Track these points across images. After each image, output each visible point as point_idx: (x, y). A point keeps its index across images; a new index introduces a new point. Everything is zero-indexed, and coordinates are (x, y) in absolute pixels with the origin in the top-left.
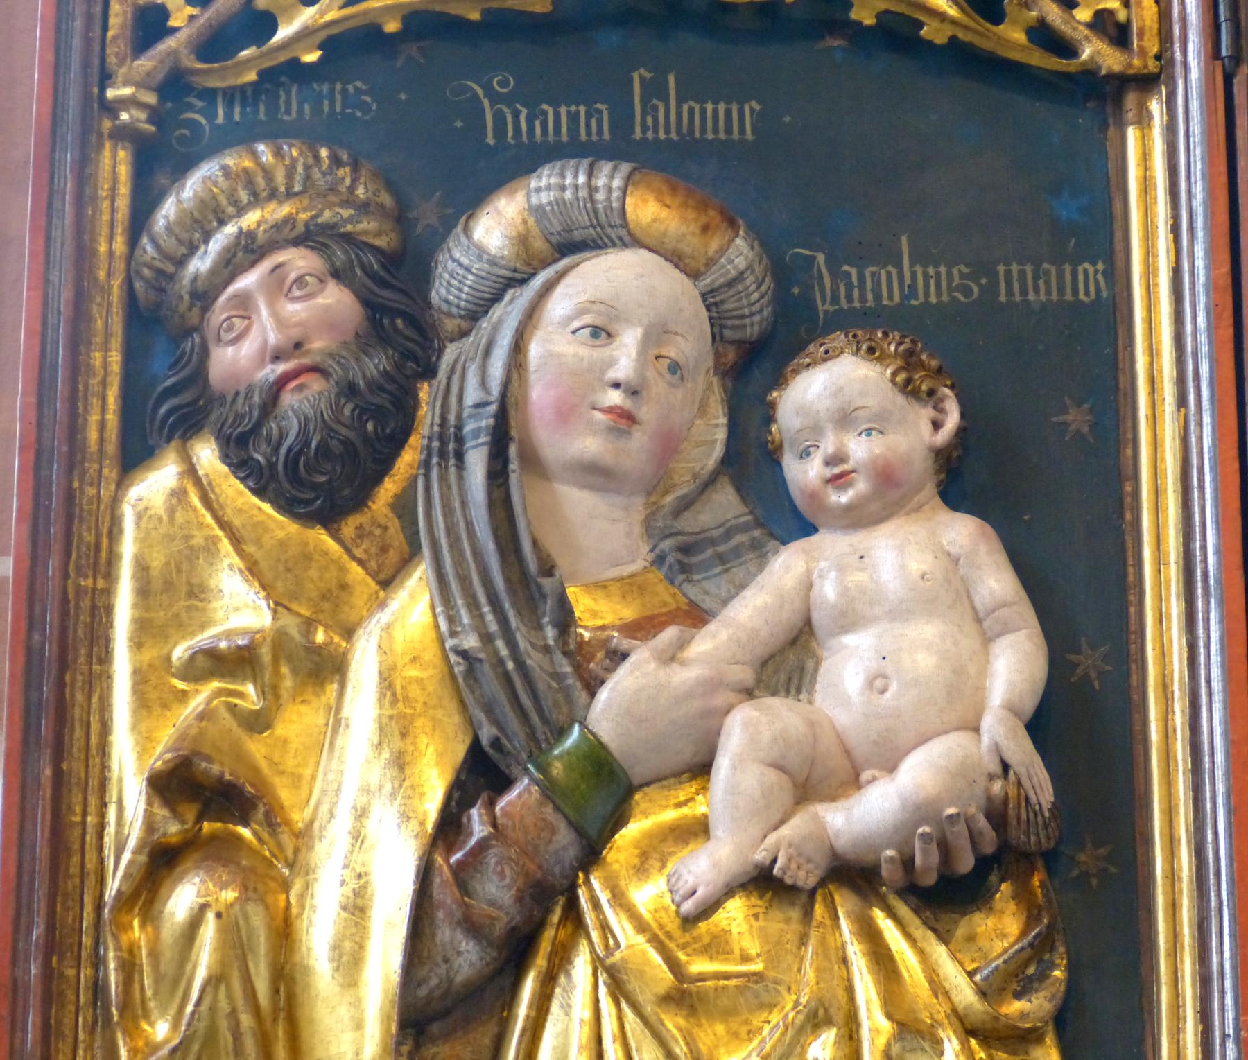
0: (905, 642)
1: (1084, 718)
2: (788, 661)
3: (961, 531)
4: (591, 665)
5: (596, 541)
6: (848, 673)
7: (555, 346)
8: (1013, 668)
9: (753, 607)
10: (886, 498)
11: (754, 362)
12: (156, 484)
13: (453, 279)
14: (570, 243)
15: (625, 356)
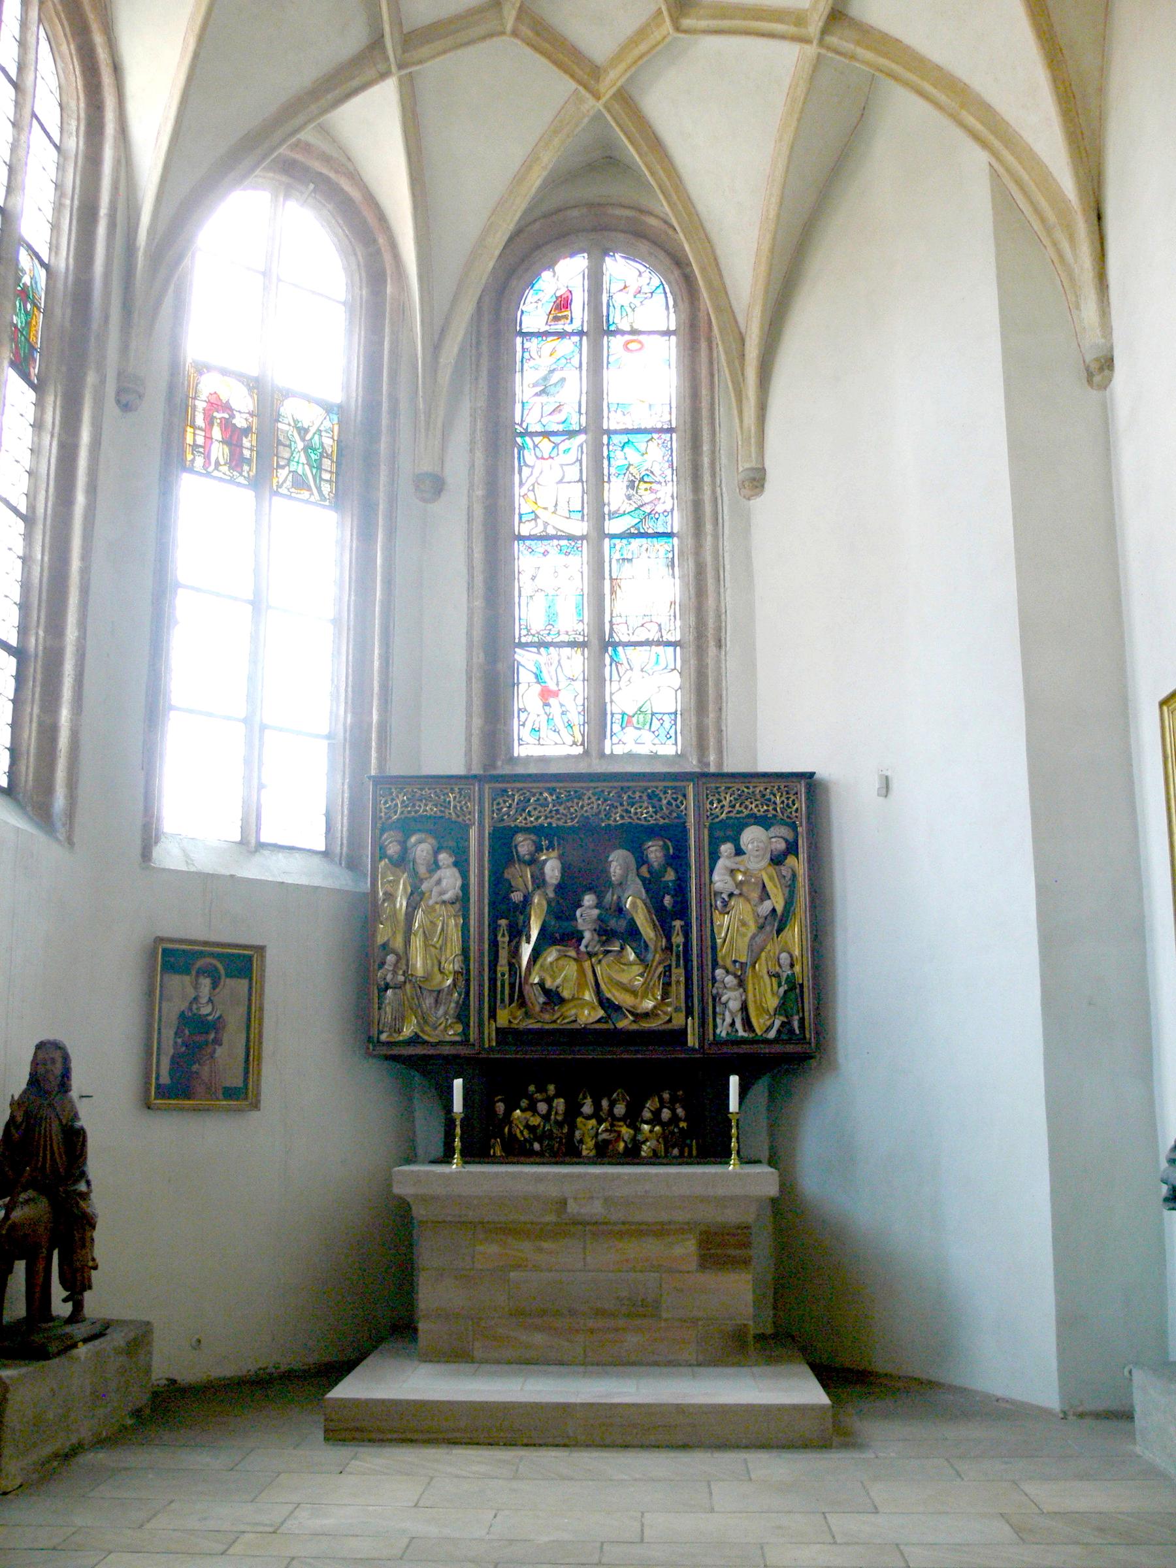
0: (450, 880)
1: (465, 887)
2: (439, 882)
3: (455, 871)
4: (421, 881)
5: (422, 870)
6: (444, 883)
7: (418, 853)
8: (459, 883)
9: (436, 877)
10: (448, 866)
11: (436, 853)
12: (383, 863)
13: (409, 844)
14: (420, 842)
15: (425, 854)
